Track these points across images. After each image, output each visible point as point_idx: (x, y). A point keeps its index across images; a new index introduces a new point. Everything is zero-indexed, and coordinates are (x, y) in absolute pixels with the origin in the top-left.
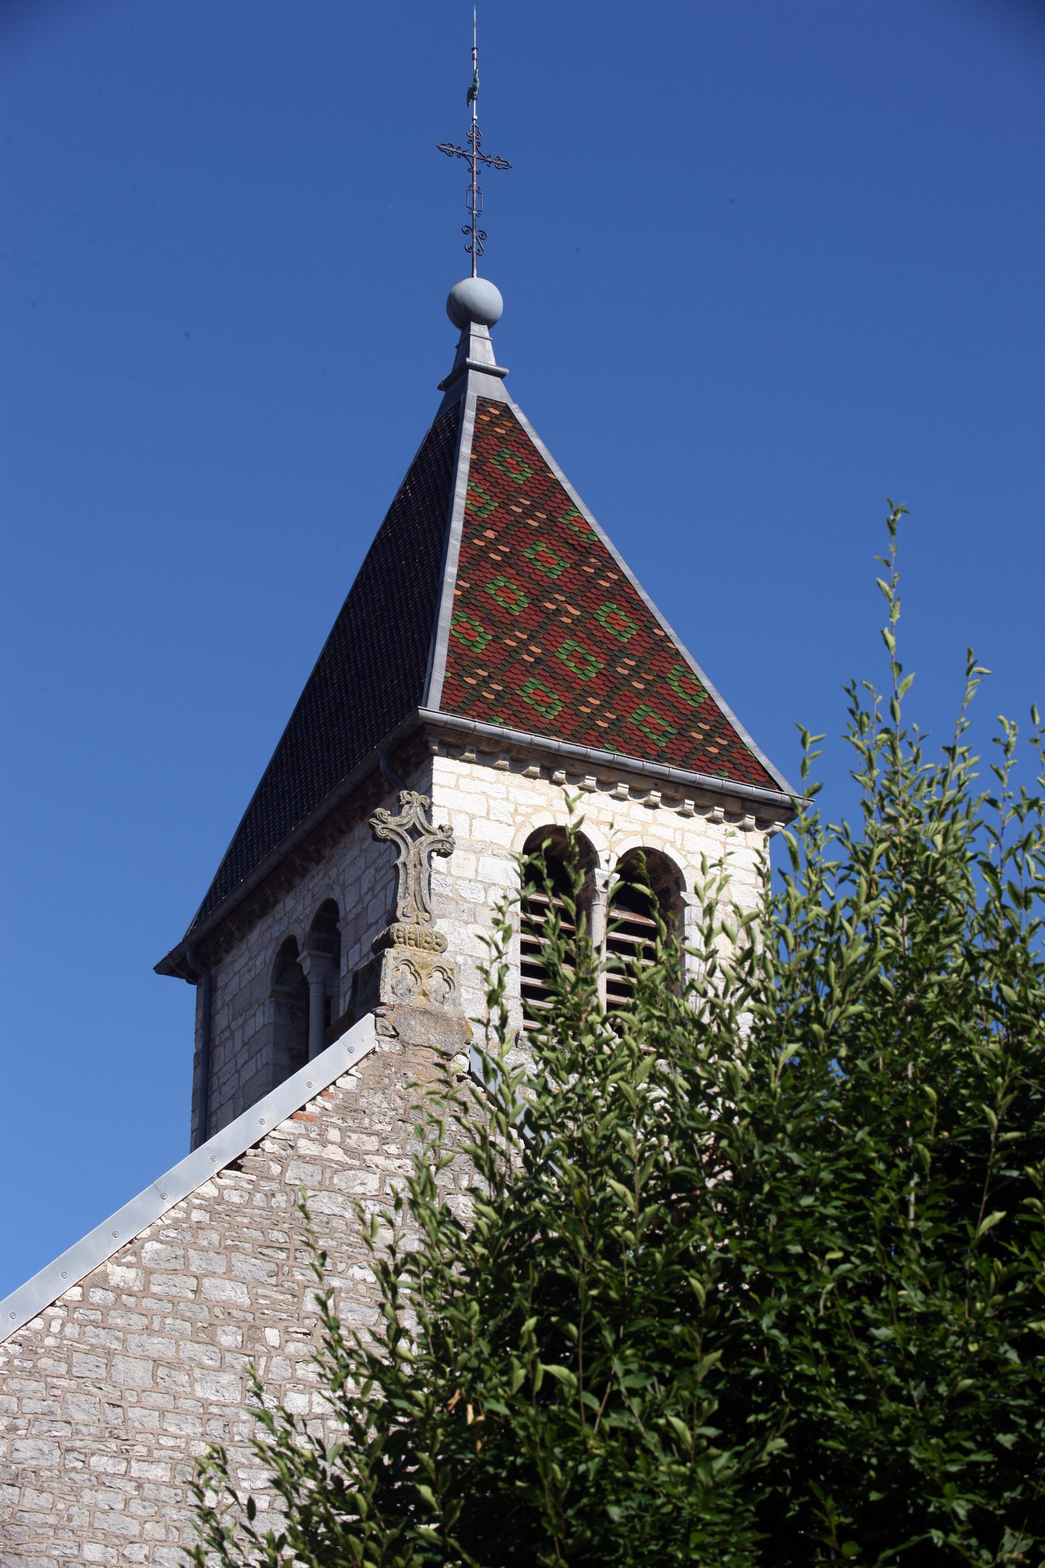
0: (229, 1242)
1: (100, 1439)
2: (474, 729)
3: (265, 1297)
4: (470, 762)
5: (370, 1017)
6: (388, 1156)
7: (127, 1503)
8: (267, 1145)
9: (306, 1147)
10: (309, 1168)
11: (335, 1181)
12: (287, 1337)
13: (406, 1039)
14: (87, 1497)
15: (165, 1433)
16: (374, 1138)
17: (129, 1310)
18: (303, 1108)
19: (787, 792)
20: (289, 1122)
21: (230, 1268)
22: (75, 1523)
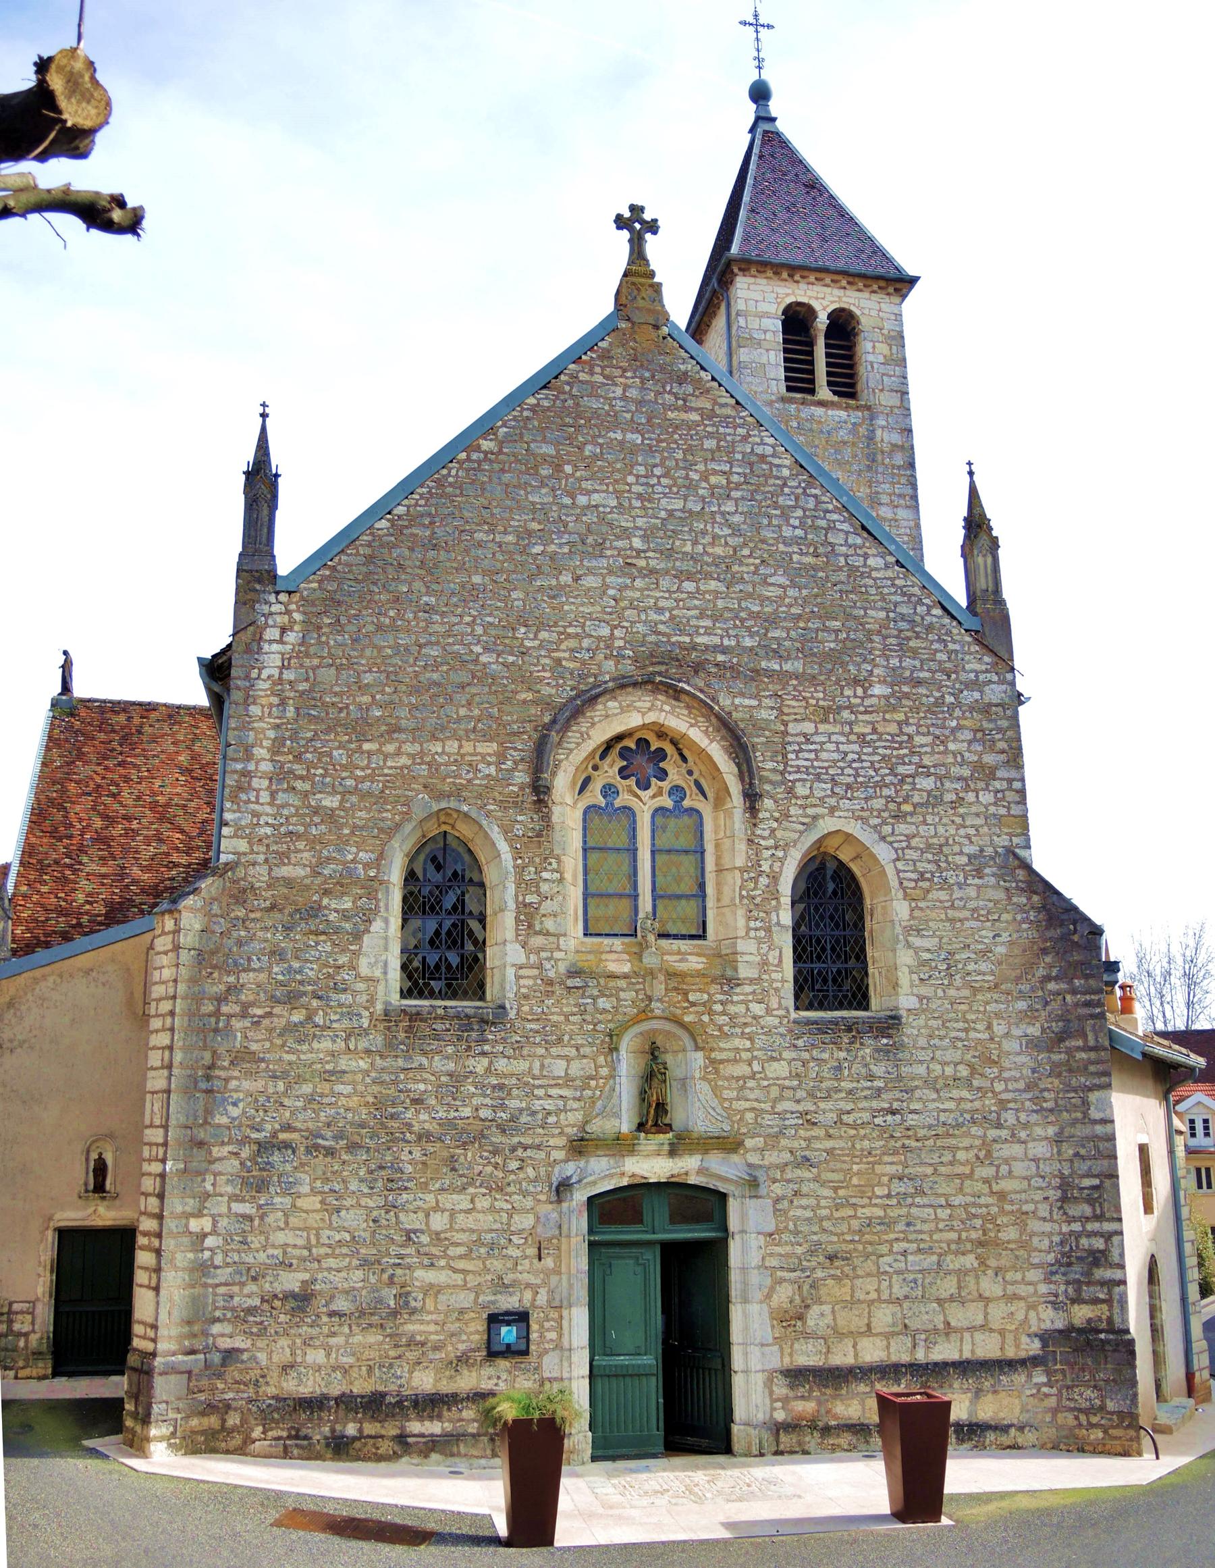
1: (478, 525)
6: (627, 378)
7: (494, 554)
8: (562, 377)
9: (583, 376)
14: (473, 552)
15: (513, 519)
17: (491, 461)
22: (467, 565)
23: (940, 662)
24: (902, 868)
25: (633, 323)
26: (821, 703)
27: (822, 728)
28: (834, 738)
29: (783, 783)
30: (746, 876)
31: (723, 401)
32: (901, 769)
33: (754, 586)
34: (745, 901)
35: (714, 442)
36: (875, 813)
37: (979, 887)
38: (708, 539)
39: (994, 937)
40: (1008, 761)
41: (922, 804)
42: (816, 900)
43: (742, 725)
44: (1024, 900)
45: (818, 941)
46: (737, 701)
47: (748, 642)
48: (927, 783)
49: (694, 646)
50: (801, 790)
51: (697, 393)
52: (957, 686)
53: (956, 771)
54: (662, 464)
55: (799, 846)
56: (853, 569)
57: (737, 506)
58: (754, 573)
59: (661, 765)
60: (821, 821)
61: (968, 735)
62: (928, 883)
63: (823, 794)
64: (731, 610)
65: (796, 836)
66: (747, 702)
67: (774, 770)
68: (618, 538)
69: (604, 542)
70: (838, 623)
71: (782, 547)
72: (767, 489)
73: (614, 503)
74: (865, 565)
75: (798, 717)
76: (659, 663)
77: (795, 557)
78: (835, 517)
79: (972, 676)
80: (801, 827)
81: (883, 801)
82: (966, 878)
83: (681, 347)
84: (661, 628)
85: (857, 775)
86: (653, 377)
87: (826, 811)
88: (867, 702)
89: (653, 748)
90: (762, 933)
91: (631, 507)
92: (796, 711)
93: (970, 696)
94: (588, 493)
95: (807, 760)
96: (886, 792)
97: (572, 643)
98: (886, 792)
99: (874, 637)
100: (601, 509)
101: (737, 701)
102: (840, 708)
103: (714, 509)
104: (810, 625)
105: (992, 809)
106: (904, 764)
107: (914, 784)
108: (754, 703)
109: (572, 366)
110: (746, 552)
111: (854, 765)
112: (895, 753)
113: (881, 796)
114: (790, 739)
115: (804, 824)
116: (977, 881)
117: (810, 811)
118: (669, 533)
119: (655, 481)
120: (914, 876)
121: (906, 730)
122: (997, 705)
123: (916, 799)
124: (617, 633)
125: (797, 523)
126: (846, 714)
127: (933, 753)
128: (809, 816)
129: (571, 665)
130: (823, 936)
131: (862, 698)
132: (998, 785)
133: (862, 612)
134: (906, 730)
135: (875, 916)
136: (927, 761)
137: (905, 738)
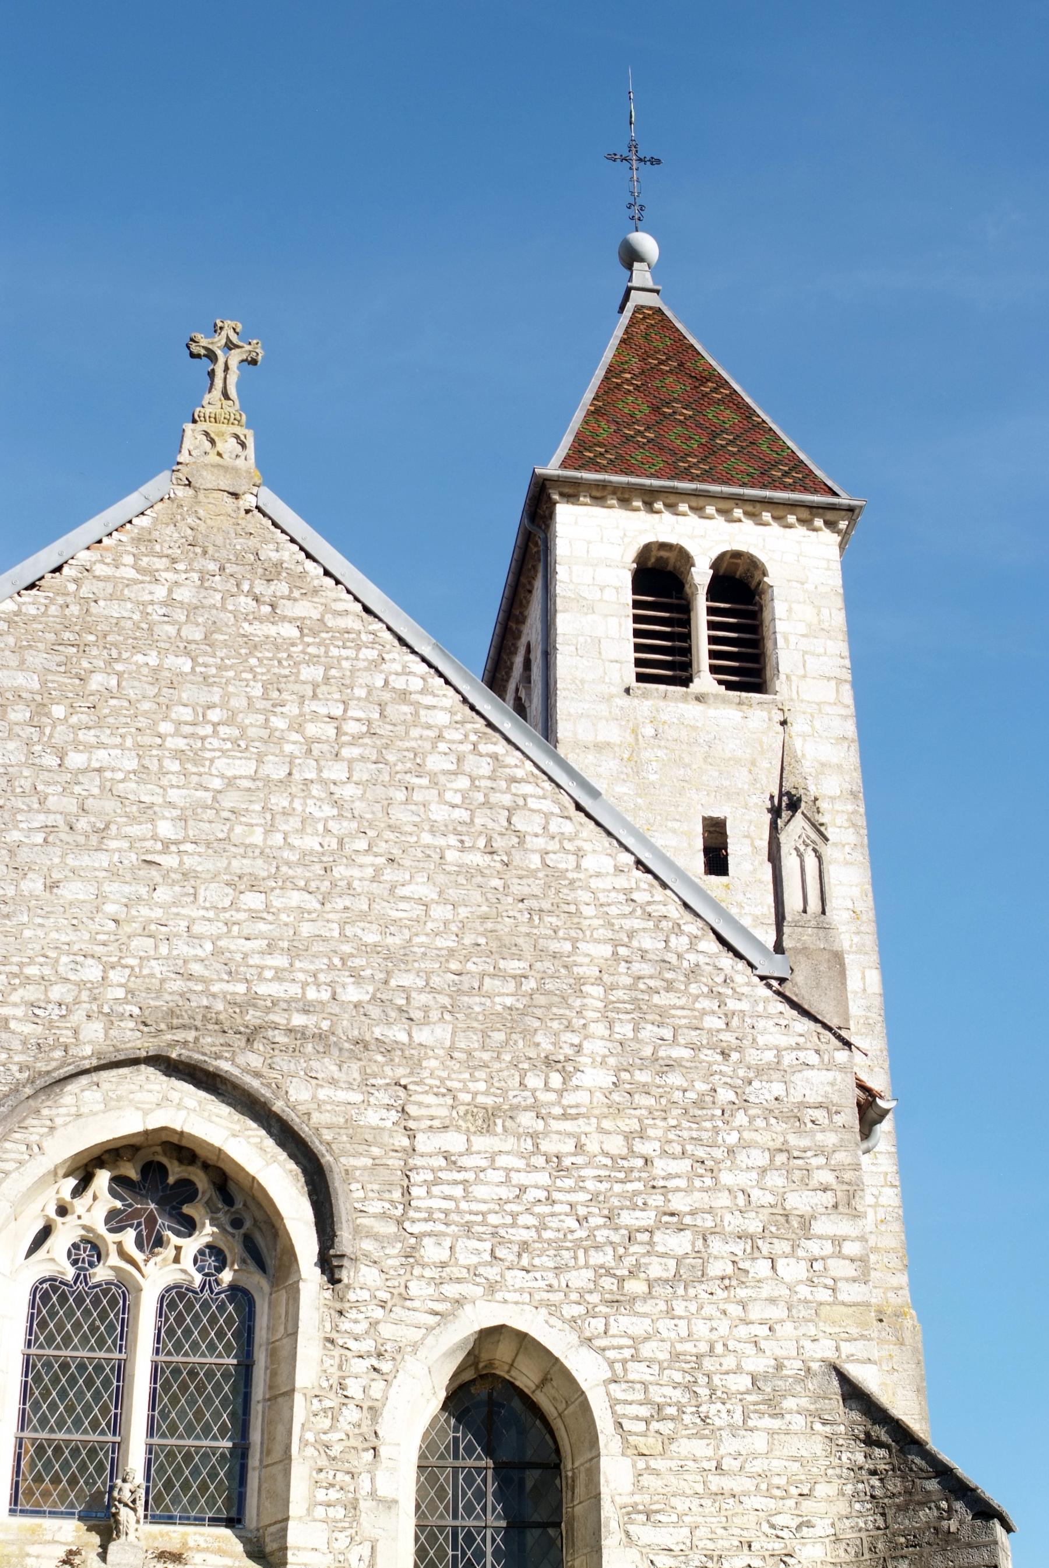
0: (25, 643)
2: (582, 478)
3: (53, 681)
4: (586, 504)
5: (167, 474)
8: (66, 570)
9: (100, 570)
10: (101, 584)
11: (126, 592)
12: (71, 710)
13: (198, 485)
16: (164, 559)
18: (100, 541)
19: (844, 500)
20: (87, 552)
21: (23, 662)
23: (710, 1031)
24: (621, 1396)
25: (196, 490)
26: (481, 1099)
27: (480, 1142)
28: (502, 1161)
29: (397, 1238)
30: (316, 1405)
31: (340, 606)
32: (627, 1218)
33: (371, 901)
34: (310, 1451)
35: (321, 671)
36: (574, 1296)
37: (772, 1433)
38: (294, 823)
39: (799, 1527)
40: (836, 1206)
41: (667, 1281)
42: (470, 1462)
43: (327, 1136)
44: (860, 1458)
45: (469, 1539)
46: (322, 1094)
47: (352, 994)
48: (680, 1243)
49: (252, 1001)
50: (432, 1251)
51: (296, 594)
52: (741, 1073)
53: (732, 1222)
54: (224, 704)
55: (422, 1353)
56: (555, 875)
57: (350, 770)
58: (374, 880)
59: (187, 1209)
60: (468, 1307)
61: (760, 1159)
62: (671, 1425)
63: (474, 1260)
64: (325, 940)
65: (416, 1335)
66: (342, 1095)
67: (384, 1216)
68: (133, 820)
69: (107, 827)
70: (522, 964)
71: (426, 838)
72: (407, 744)
73: (132, 764)
74: (578, 866)
75: (436, 1123)
76: (184, 1027)
77: (451, 856)
78: (527, 789)
79: (769, 1056)
80: (432, 1320)
81: (590, 1274)
82: (746, 1417)
83: (275, 525)
84: (196, 968)
85: (542, 1227)
86: (222, 569)
87: (479, 1291)
88: (569, 1099)
89: (171, 1180)
90: (339, 1512)
91: (163, 772)
92: (432, 1112)
93: (765, 1091)
94: (89, 748)
95: (445, 1198)
96: (597, 1258)
97: (32, 993)
98: (597, 1258)
99: (587, 989)
100: (108, 775)
101: (322, 1094)
102: (514, 1108)
103: (312, 775)
104: (470, 966)
105: (804, 1291)
106: (634, 1207)
107: (651, 1243)
108: (356, 1097)
109: (84, 556)
110: (362, 844)
111: (537, 1209)
112: (618, 1188)
113: (587, 1266)
114: (418, 1161)
115: (437, 1314)
116: (767, 1422)
117: (451, 1290)
118: (225, 814)
119: (209, 730)
120: (644, 1411)
121: (640, 1147)
122: (819, 1106)
123: (656, 1270)
124: (113, 975)
125: (457, 799)
126: (527, 1119)
127: (689, 1190)
128: (445, 1299)
129: (28, 1029)
130: (479, 1529)
131: (560, 1093)
132: (814, 1247)
133: (567, 947)
134: (640, 1147)
135: (577, 1491)
136: (678, 1203)
137: (640, 1162)
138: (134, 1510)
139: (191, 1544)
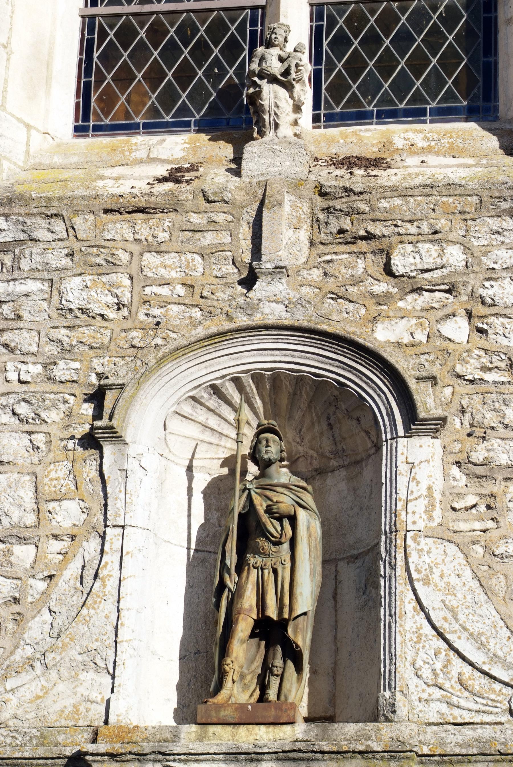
138: (288, 87)
139: (399, 143)
